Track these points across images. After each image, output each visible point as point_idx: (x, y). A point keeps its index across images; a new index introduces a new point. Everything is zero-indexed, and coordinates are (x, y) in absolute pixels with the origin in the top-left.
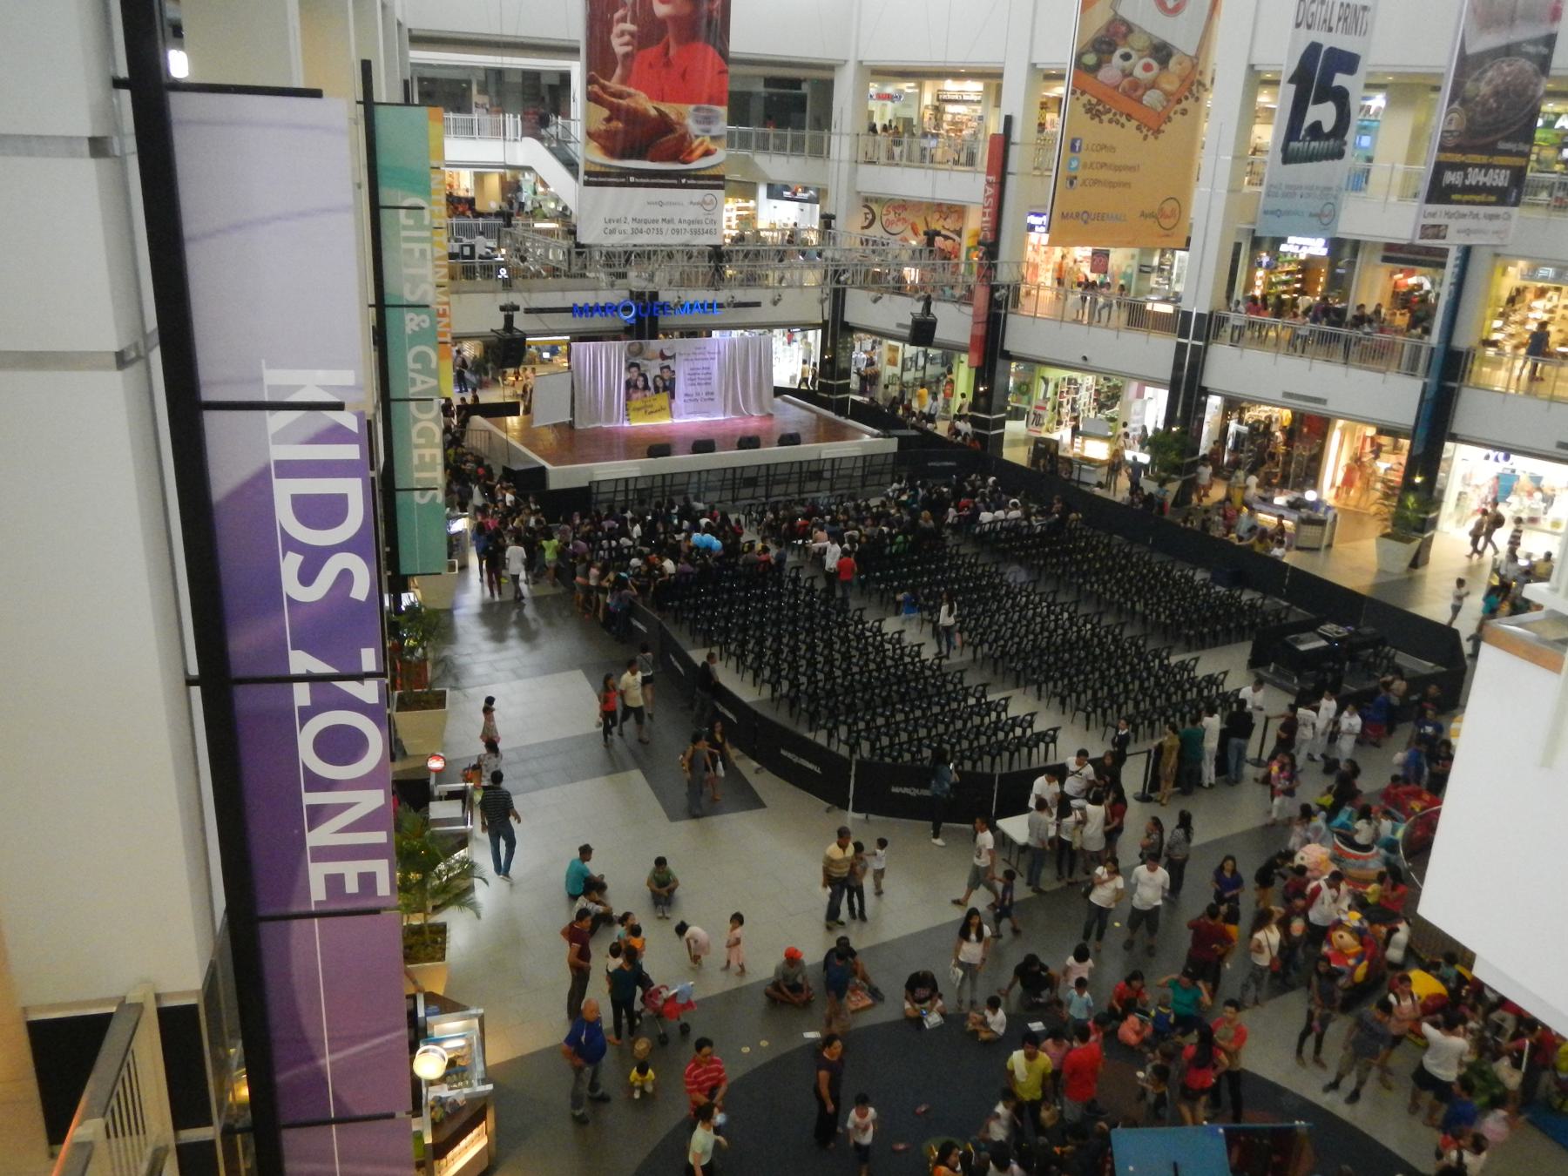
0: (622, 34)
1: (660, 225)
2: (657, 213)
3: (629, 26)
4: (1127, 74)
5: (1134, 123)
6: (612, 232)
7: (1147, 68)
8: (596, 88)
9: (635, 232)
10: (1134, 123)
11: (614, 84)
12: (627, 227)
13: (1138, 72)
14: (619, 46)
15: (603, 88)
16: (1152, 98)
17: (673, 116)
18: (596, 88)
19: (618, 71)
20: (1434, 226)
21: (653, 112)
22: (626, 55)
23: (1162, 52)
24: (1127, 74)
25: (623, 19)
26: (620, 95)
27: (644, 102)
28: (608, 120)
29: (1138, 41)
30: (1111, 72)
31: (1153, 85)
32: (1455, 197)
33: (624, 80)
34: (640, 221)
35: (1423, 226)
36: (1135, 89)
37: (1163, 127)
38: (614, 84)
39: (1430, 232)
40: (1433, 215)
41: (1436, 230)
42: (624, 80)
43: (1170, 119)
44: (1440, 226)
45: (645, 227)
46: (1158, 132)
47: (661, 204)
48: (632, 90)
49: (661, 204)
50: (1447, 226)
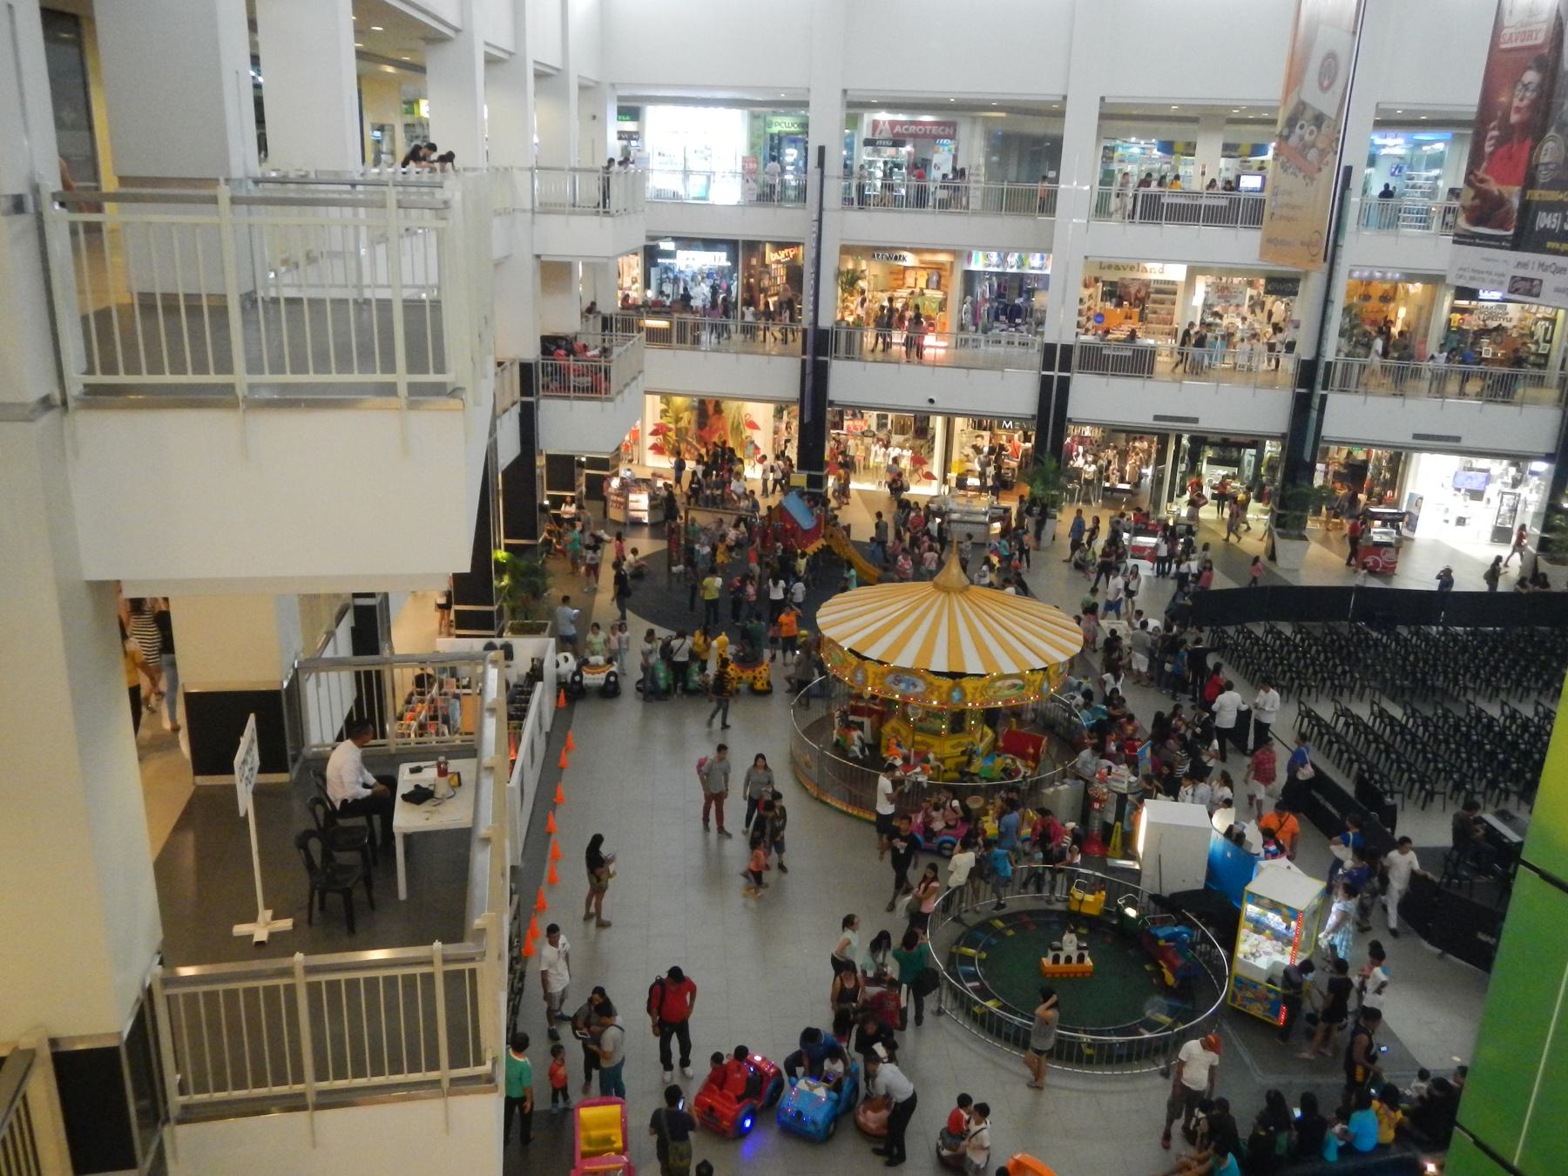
0: (1492, 138)
1: (1485, 276)
2: (1484, 266)
3: (1495, 133)
4: (1302, 138)
5: (1302, 175)
6: (1461, 277)
7: (1311, 133)
8: (1472, 177)
9: (1472, 278)
10: (1302, 175)
11: (1480, 174)
12: (1468, 274)
13: (1307, 137)
14: (1488, 148)
15: (1476, 176)
16: (1312, 155)
17: (1506, 195)
18: (1472, 177)
19: (1484, 165)
20: (1524, 279)
21: (1496, 193)
22: (1492, 153)
23: (1319, 119)
24: (1302, 138)
25: (1493, 129)
26: (1482, 181)
27: (1494, 187)
28: (1474, 198)
29: (1309, 115)
30: (1294, 140)
31: (1313, 145)
32: (1550, 245)
33: (1486, 171)
34: (1465, 270)
35: (1514, 277)
36: (1305, 147)
37: (1316, 176)
38: (1480, 174)
39: (1521, 285)
40: (1524, 265)
41: (1527, 285)
42: (1486, 171)
43: (1320, 170)
44: (1532, 280)
45: (1477, 275)
46: (1312, 179)
47: (1488, 260)
48: (1488, 177)
49: (1488, 260)
50: (1541, 281)
